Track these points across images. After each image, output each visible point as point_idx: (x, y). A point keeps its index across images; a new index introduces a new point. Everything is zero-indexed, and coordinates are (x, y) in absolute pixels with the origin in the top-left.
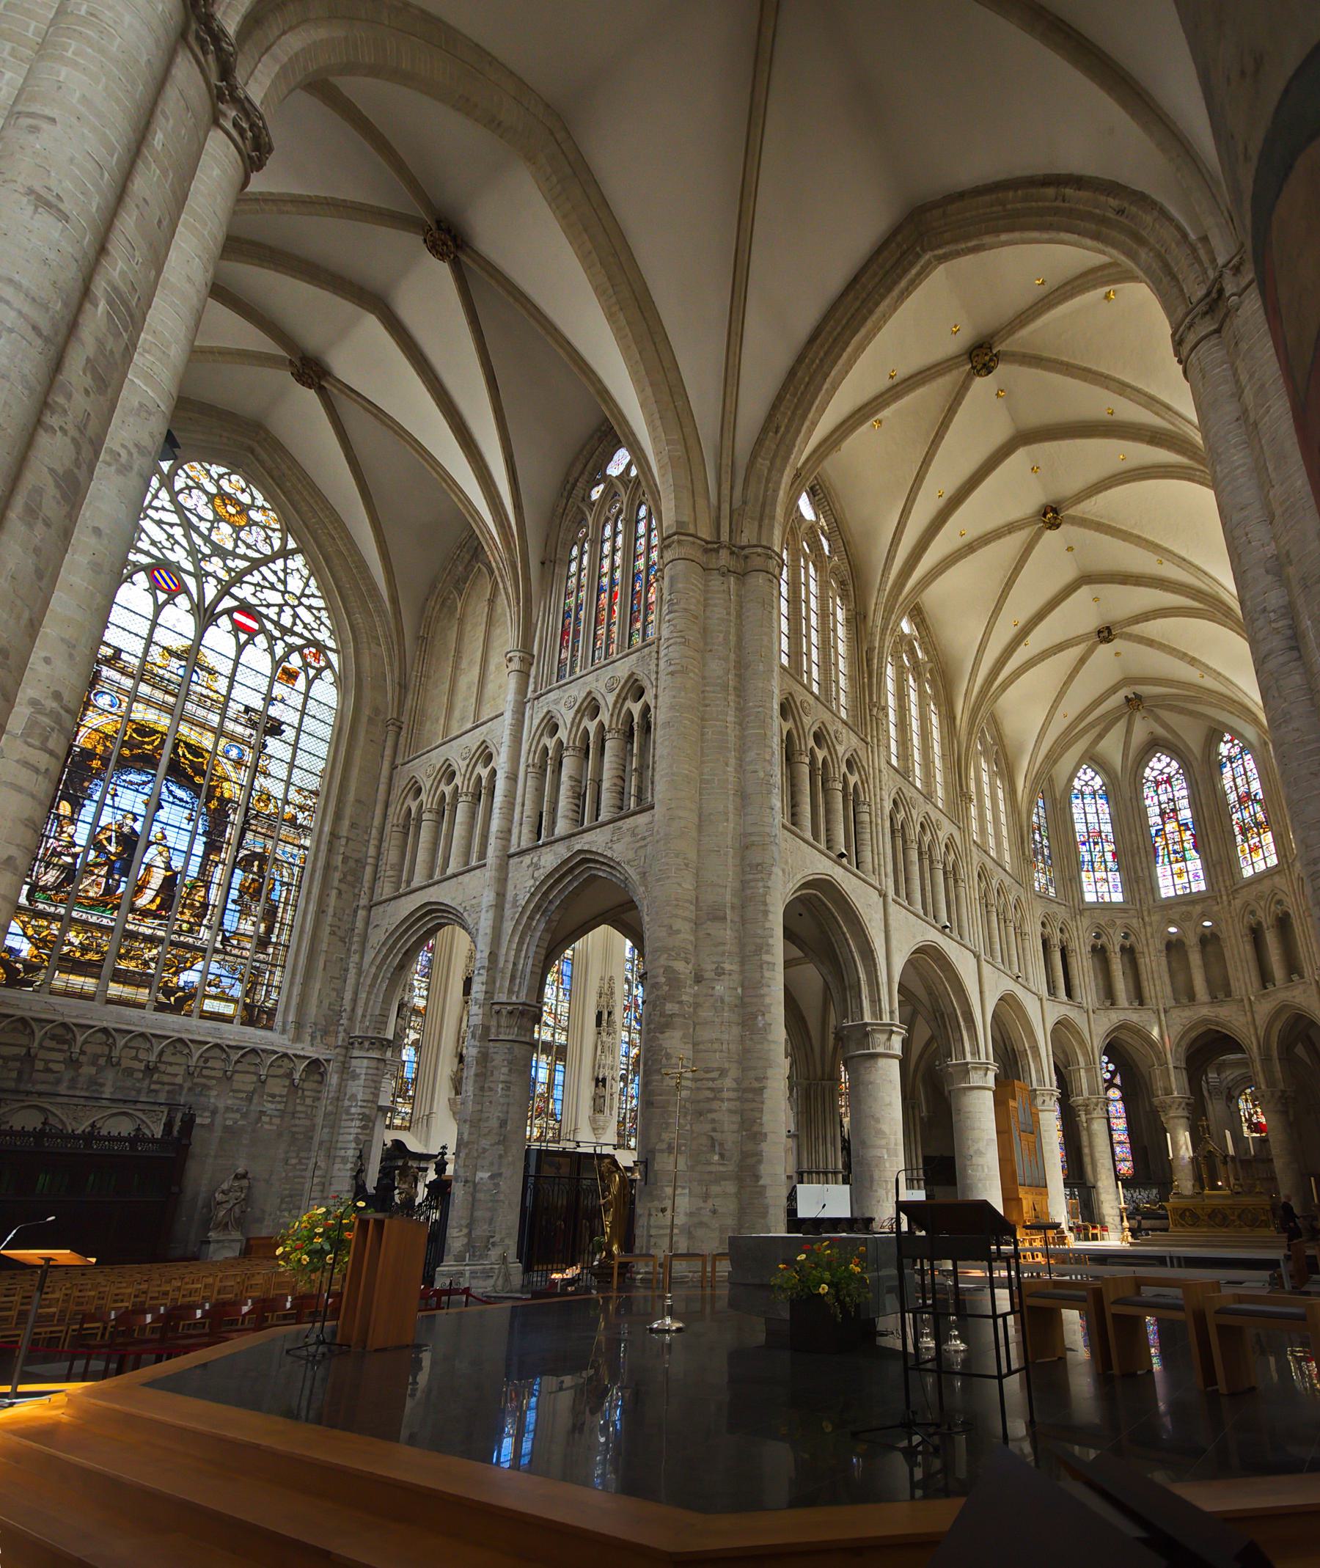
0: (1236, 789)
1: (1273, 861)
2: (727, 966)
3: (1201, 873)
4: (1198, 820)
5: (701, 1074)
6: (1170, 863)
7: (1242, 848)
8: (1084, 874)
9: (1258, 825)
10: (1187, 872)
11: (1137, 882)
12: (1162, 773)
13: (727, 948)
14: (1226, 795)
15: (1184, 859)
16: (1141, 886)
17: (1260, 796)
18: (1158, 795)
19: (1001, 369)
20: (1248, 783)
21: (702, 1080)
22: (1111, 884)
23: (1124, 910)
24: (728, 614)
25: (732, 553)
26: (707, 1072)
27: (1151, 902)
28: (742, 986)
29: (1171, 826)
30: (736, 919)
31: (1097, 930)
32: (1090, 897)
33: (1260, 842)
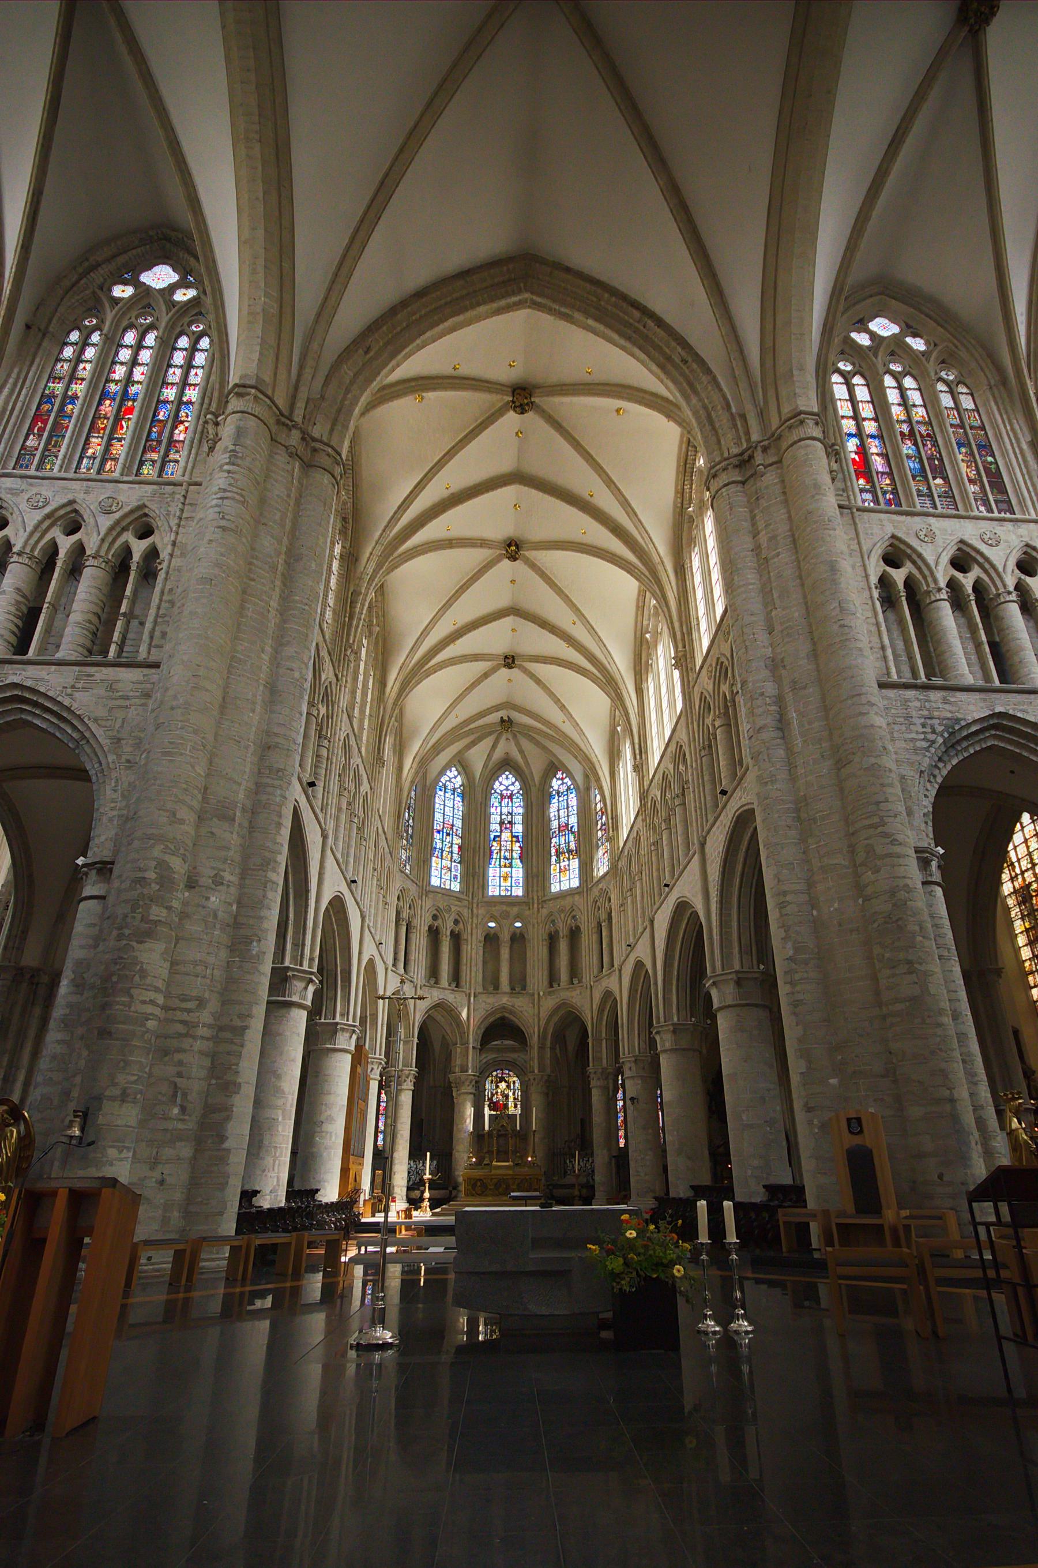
1: (575, 883)
2: (227, 876)
4: (527, 836)
5: (176, 1003)
6: (500, 867)
7: (554, 869)
8: (434, 859)
9: (570, 851)
10: (511, 877)
11: (473, 877)
13: (231, 853)
16: (476, 882)
17: (575, 829)
19: (530, 415)
21: (175, 1009)
22: (453, 873)
23: (459, 900)
24: (289, 496)
25: (303, 439)
26: (183, 1000)
27: (481, 896)
28: (239, 903)
29: (506, 836)
30: (246, 824)
31: (435, 912)
32: (435, 882)
33: (569, 865)
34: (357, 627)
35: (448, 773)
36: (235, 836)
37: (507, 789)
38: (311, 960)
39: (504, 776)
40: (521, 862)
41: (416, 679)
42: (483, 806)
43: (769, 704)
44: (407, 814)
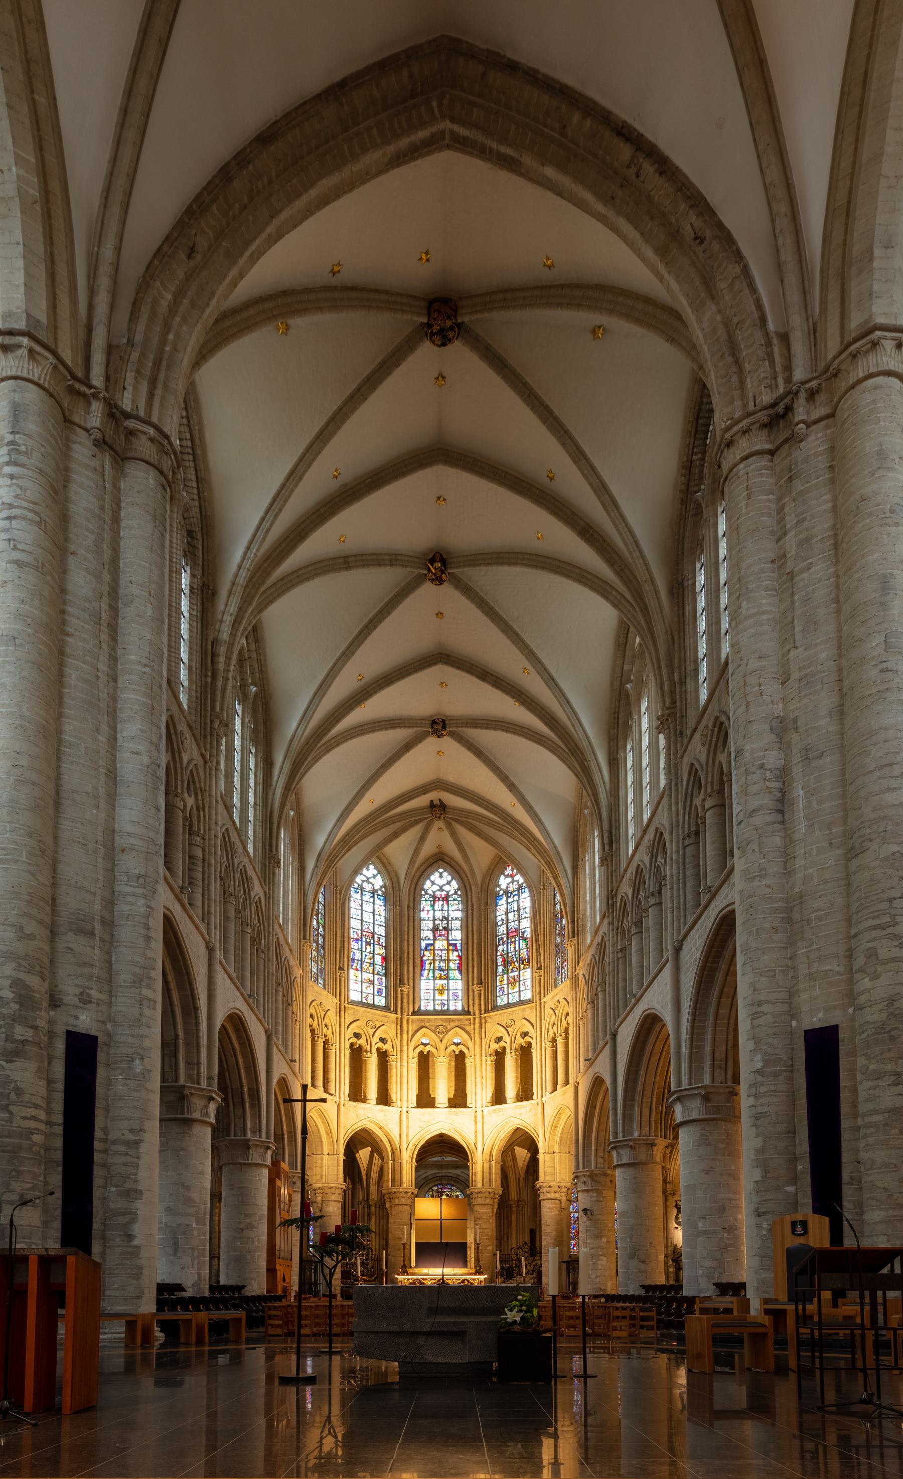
0: (507, 923)
3: (460, 993)
4: (467, 944)
6: (434, 978)
7: (502, 980)
8: (352, 972)
9: (521, 960)
10: (448, 990)
12: (441, 890)
14: (497, 925)
15: (447, 978)
17: (528, 934)
18: (434, 910)
20: (519, 920)
22: (376, 987)
29: (440, 944)
33: (519, 976)
34: (224, 690)
35: (365, 871)
36: (97, 952)
37: (441, 890)
38: (210, 1078)
39: (437, 874)
40: (461, 973)
41: (313, 754)
42: (411, 909)
43: (769, 780)
44: (315, 922)
